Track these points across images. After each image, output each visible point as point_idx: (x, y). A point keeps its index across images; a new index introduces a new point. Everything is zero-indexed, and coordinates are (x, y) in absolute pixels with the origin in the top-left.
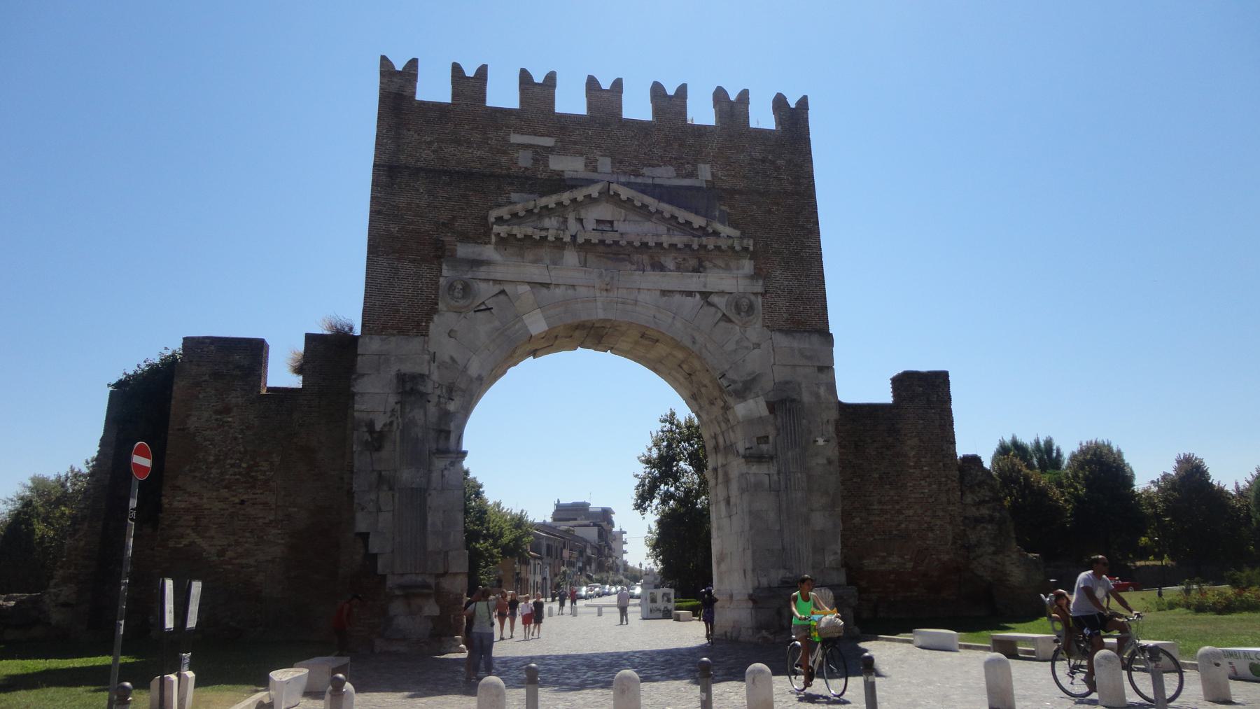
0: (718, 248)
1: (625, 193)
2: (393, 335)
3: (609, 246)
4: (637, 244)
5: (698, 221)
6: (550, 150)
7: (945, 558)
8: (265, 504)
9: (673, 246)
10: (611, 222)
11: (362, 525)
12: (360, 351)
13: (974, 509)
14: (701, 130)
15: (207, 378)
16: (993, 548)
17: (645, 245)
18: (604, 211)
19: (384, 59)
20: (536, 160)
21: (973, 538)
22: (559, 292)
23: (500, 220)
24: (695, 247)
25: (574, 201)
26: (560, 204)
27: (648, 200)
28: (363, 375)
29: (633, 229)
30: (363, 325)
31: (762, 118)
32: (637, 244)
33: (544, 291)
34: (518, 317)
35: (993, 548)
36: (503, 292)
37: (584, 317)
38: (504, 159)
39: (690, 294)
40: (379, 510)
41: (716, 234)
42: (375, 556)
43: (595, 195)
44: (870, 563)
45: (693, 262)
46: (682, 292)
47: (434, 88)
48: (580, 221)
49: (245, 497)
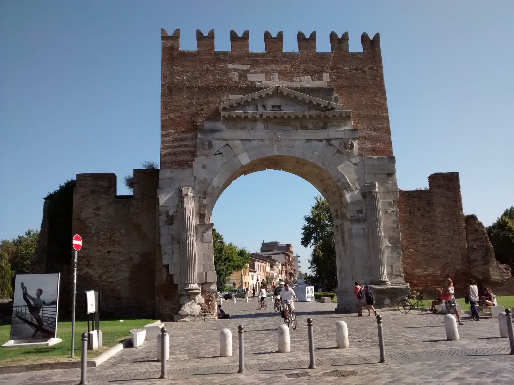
0: (334, 116)
2: (175, 168)
3: (279, 118)
4: (293, 117)
6: (248, 71)
7: (457, 268)
8: (119, 252)
9: (311, 117)
10: (280, 107)
11: (165, 262)
12: (160, 178)
13: (473, 242)
14: (323, 55)
15: (88, 193)
17: (297, 118)
19: (163, 30)
20: (240, 78)
21: (473, 256)
22: (255, 143)
23: (224, 109)
24: (322, 116)
25: (260, 97)
26: (253, 99)
27: (298, 93)
28: (162, 188)
29: (289, 110)
30: (161, 165)
31: (355, 46)
32: (293, 117)
33: (248, 143)
34: (235, 156)
35: (483, 262)
36: (228, 145)
37: (268, 155)
39: (321, 140)
40: (173, 253)
41: (333, 109)
42: (172, 275)
43: (271, 93)
44: (418, 272)
45: (322, 124)
46: (316, 140)
47: (188, 44)
48: (264, 107)
49: (110, 250)
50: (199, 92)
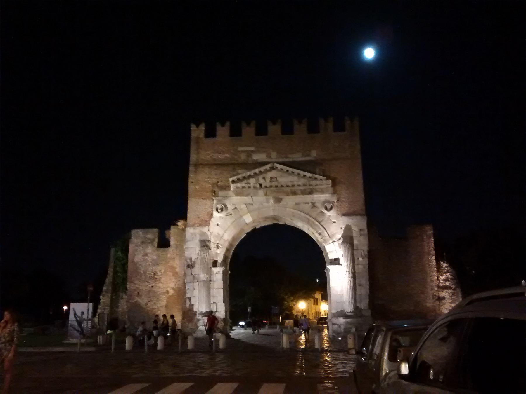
1: (279, 166)
5: (308, 175)
6: (252, 151)
10: (276, 178)
11: (188, 295)
16: (450, 301)
18: (273, 174)
23: (233, 182)
36: (236, 208)
38: (236, 157)
39: (308, 203)
40: (194, 289)
41: (316, 179)
48: (264, 178)
50: (216, 169)
